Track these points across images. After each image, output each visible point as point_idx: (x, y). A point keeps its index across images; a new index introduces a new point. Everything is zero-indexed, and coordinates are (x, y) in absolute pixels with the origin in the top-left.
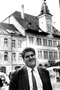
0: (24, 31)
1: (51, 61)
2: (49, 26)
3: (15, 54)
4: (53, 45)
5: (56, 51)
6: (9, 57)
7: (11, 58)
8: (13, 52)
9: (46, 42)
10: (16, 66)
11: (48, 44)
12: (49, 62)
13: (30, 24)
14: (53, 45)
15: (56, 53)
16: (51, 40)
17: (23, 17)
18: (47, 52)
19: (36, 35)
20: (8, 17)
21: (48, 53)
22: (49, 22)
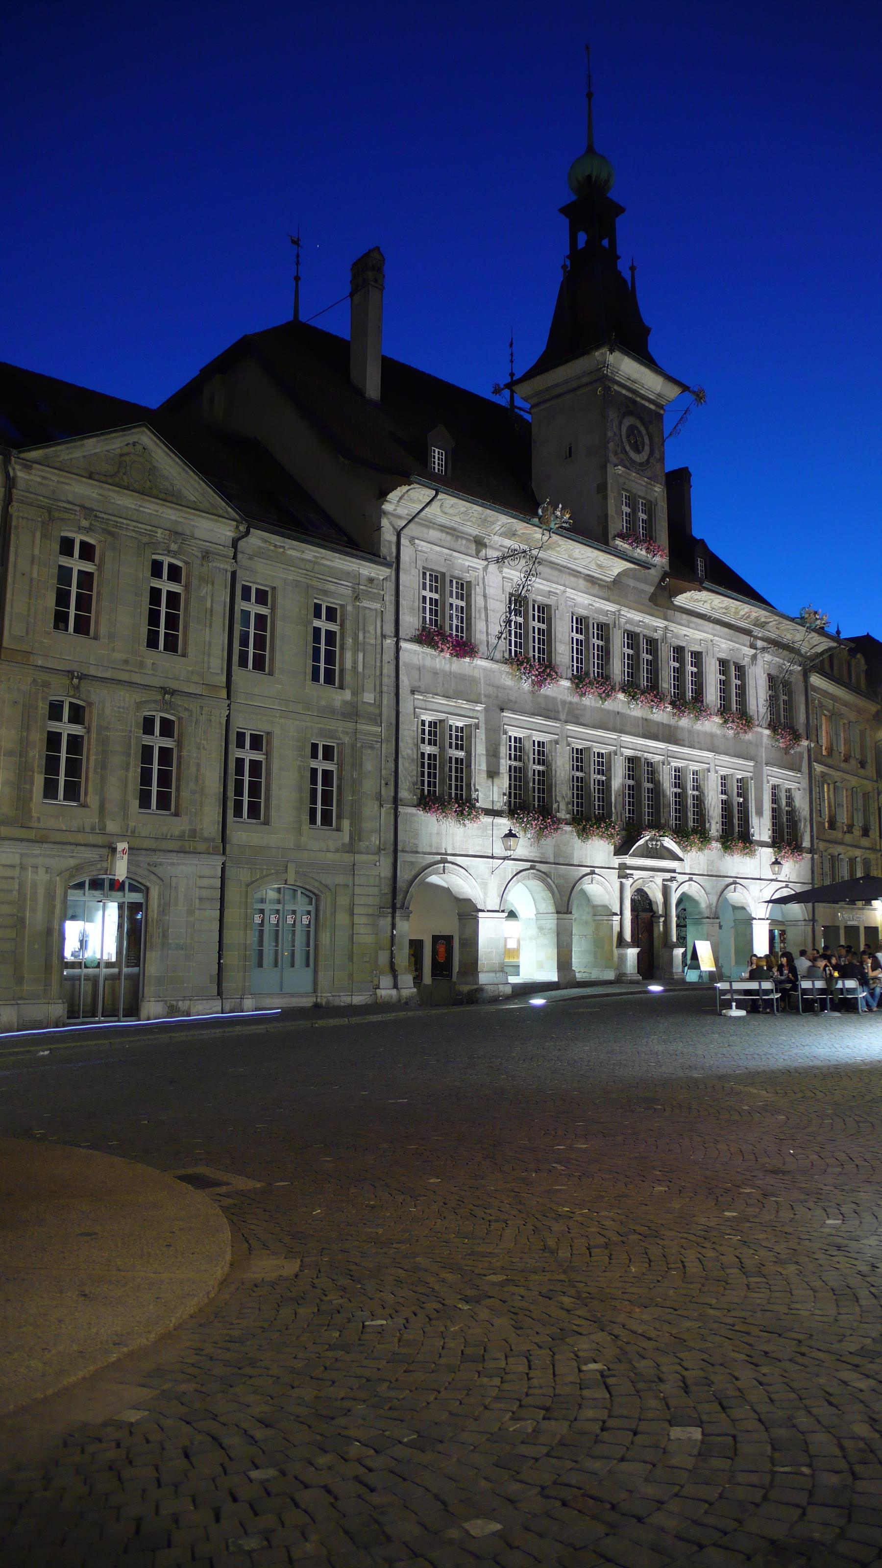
3: (257, 743)
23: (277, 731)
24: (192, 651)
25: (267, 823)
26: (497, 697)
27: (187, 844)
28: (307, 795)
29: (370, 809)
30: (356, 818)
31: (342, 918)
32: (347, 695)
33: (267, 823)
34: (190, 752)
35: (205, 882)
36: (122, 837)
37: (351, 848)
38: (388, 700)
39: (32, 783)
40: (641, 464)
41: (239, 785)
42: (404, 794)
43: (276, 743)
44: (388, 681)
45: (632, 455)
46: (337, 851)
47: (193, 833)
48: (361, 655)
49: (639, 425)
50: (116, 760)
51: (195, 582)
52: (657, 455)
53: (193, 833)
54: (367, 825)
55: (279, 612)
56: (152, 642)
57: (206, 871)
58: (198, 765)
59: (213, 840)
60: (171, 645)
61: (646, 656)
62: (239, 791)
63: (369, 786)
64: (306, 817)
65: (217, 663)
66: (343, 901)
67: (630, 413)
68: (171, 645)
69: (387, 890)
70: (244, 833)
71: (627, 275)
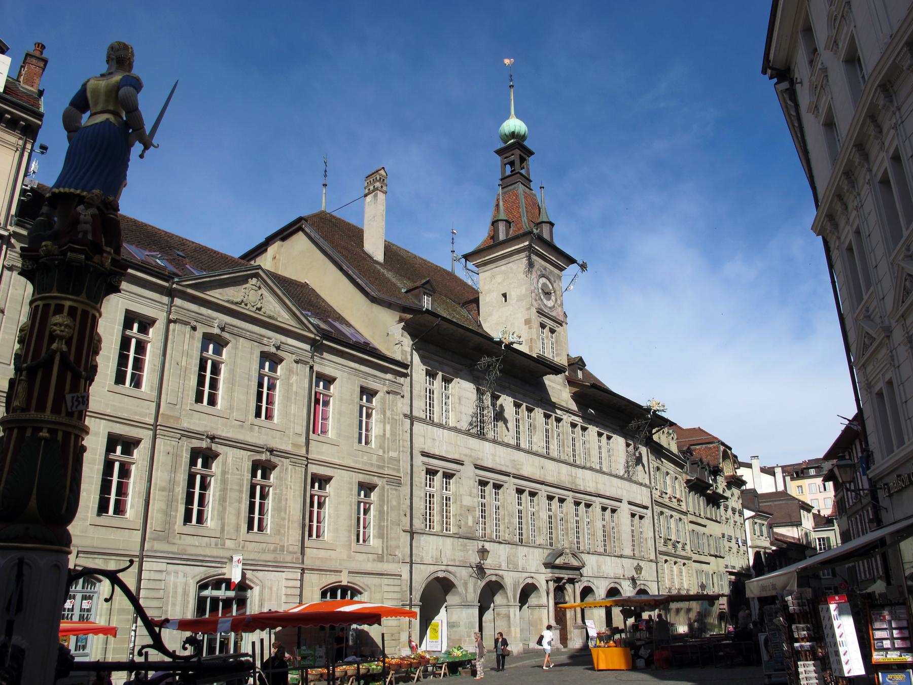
1: (558, 561)
8: (314, 469)
17: (374, 247)
26: (471, 456)
27: (278, 556)
28: (354, 522)
35: (291, 583)
36: (236, 551)
39: (177, 511)
40: (550, 308)
41: (311, 513)
45: (545, 301)
46: (374, 560)
48: (388, 427)
49: (548, 283)
50: (232, 495)
52: (559, 302)
57: (290, 576)
58: (286, 500)
59: (295, 553)
62: (311, 520)
64: (354, 537)
67: (543, 276)
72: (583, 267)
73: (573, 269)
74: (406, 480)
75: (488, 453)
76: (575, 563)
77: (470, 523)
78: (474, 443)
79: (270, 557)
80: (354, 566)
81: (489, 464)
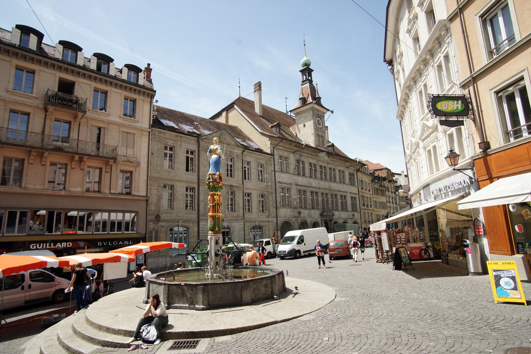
0: (269, 143)
1: (325, 214)
2: (320, 134)
3: (249, 195)
4: (328, 177)
5: (334, 191)
6: (237, 203)
7: (241, 205)
8: (245, 191)
9: (315, 170)
10: (253, 224)
11: (318, 175)
12: (322, 215)
13: (278, 126)
14: (328, 177)
15: (336, 195)
16: (324, 165)
18: (316, 193)
19: (294, 153)
20: (223, 111)
21: (320, 195)
22: (320, 125)
23: (253, 193)
24: (236, 177)
25: (251, 212)
29: (271, 208)
30: (269, 210)
31: (267, 232)
32: (266, 184)
33: (251, 212)
34: (237, 198)
37: (268, 217)
38: (274, 184)
42: (278, 205)
43: (252, 195)
44: (274, 180)
47: (238, 216)
51: (235, 162)
53: (238, 216)
54: (271, 212)
55: (251, 167)
56: (228, 176)
60: (231, 176)
61: (324, 171)
63: (271, 203)
65: (241, 179)
66: (267, 228)
68: (231, 176)
69: (276, 225)
70: (248, 216)
71: (315, 85)
72: (332, 112)
73: (329, 113)
74: (274, 192)
75: (300, 180)
76: (331, 214)
77: (295, 203)
78: (296, 177)
79: (235, 219)
80: (259, 219)
81: (301, 184)
